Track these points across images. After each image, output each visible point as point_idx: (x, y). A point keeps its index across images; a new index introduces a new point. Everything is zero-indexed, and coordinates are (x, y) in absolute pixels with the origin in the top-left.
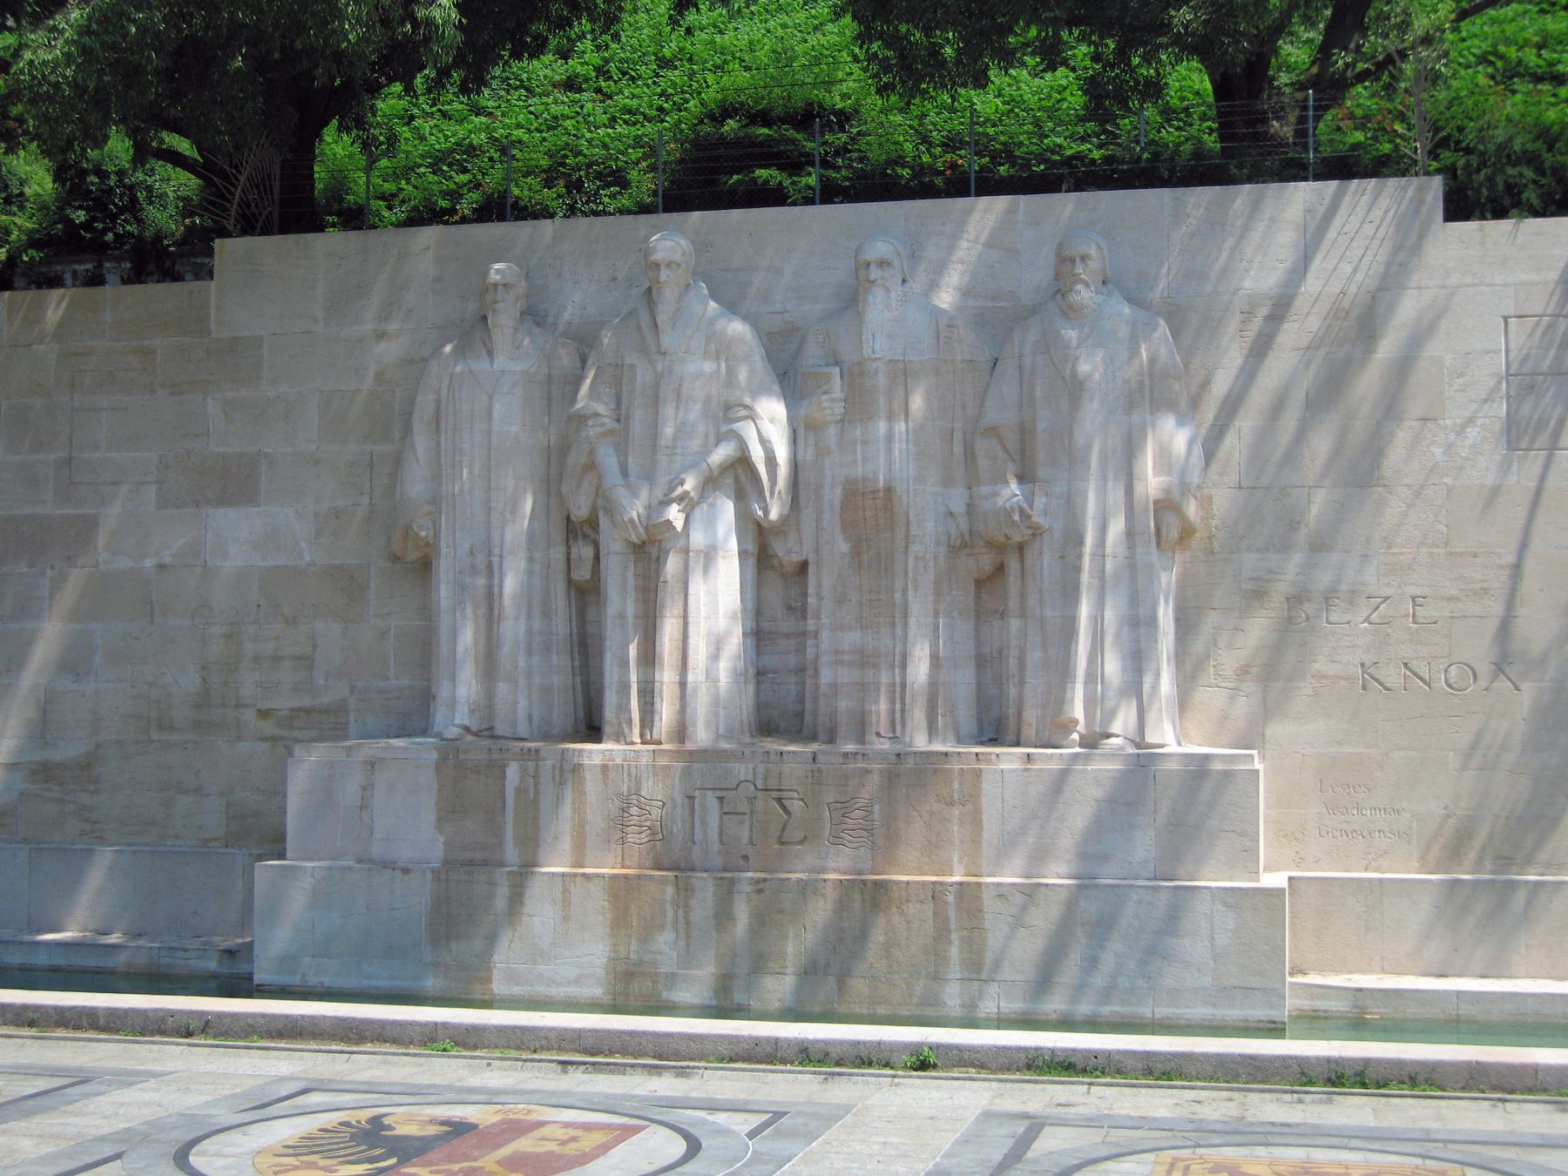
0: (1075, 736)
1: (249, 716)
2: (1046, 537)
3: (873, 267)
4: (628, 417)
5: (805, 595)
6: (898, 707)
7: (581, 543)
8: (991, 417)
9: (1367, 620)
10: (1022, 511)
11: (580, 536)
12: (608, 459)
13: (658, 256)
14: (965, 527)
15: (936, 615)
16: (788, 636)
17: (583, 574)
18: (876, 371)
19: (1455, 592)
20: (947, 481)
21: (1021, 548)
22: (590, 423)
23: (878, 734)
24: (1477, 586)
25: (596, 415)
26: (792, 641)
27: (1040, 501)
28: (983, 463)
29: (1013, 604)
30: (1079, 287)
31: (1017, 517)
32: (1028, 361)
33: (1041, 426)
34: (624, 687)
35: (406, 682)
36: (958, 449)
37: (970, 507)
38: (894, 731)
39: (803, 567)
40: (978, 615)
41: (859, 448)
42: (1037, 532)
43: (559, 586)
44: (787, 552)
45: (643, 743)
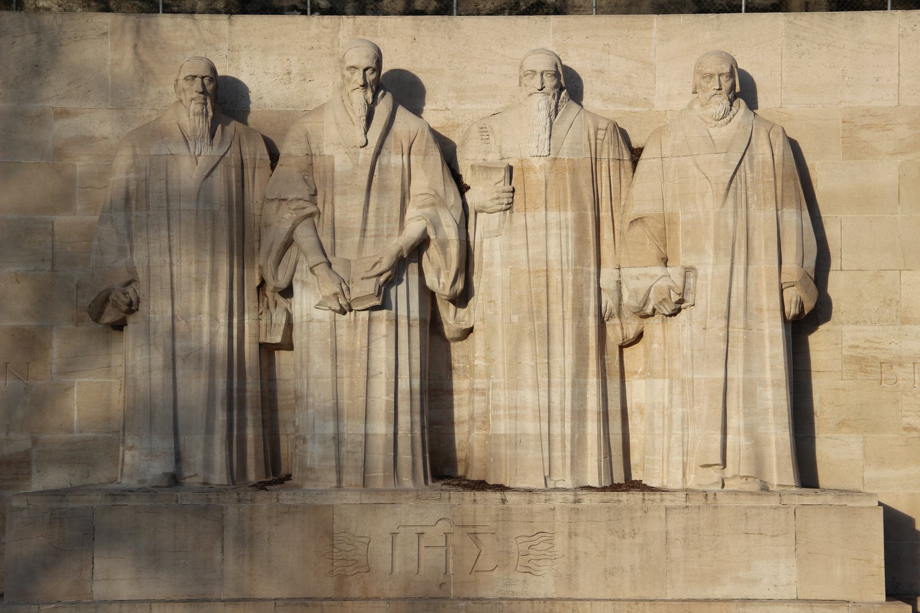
22: (294, 205)
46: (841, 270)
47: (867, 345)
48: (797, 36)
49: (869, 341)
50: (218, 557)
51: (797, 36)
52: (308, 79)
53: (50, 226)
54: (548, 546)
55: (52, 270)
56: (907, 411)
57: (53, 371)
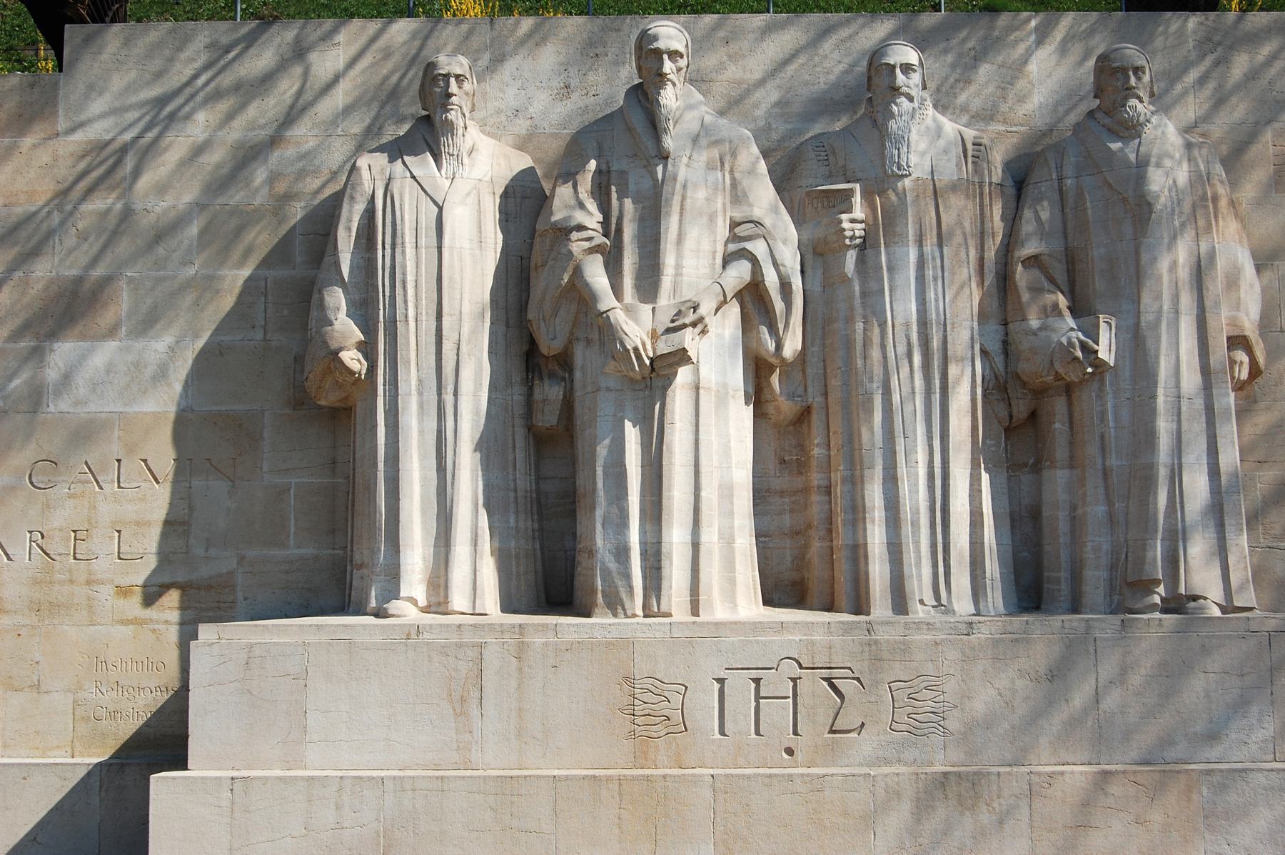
0: (1157, 599)
1: (106, 592)
4: (619, 230)
7: (547, 383)
10: (1084, 346)
11: (545, 374)
12: (597, 275)
13: (661, 44)
16: (782, 493)
17: (548, 418)
21: (1069, 389)
23: (921, 602)
25: (581, 228)
31: (1079, 354)
34: (622, 553)
35: (308, 551)
43: (520, 433)
45: (645, 616)
50: (475, 712)
52: (591, 94)
53: (263, 283)
55: (265, 339)
57: (265, 469)
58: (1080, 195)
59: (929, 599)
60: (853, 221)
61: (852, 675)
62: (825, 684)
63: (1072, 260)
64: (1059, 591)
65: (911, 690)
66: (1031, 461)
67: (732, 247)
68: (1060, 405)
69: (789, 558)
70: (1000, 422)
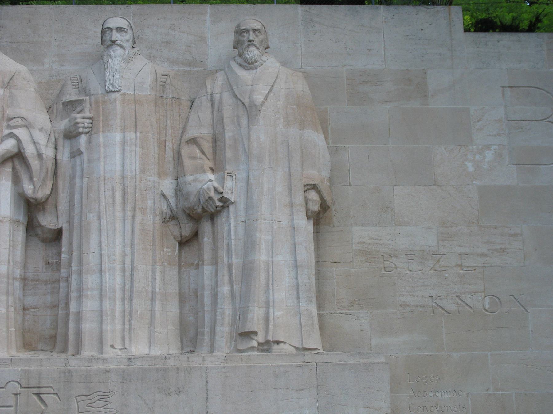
0: (255, 344)
2: (232, 208)
3: (114, 32)
5: (59, 254)
6: (127, 327)
8: (191, 133)
9: (433, 268)
10: (216, 189)
14: (173, 205)
15: (154, 263)
16: (46, 282)
18: (115, 100)
19: (485, 251)
20: (161, 174)
23: (112, 346)
24: (498, 247)
26: (49, 286)
27: (229, 183)
28: (187, 163)
29: (207, 256)
30: (252, 48)
32: (217, 96)
33: (228, 135)
36: (169, 154)
37: (178, 191)
38: (124, 344)
39: (59, 233)
40: (180, 267)
41: (102, 149)
42: (225, 203)
44: (47, 221)
46: (350, 185)
47: (371, 241)
48: (312, 20)
49: (372, 239)
51: (312, 20)
54: (104, 403)
56: (402, 292)
58: (221, 102)
59: (119, 346)
60: (84, 118)
61: (53, 391)
62: (35, 397)
63: (216, 141)
64: (203, 339)
65: (90, 401)
66: (196, 262)
67: (6, 132)
68: (206, 227)
69: (49, 322)
70: (175, 238)
